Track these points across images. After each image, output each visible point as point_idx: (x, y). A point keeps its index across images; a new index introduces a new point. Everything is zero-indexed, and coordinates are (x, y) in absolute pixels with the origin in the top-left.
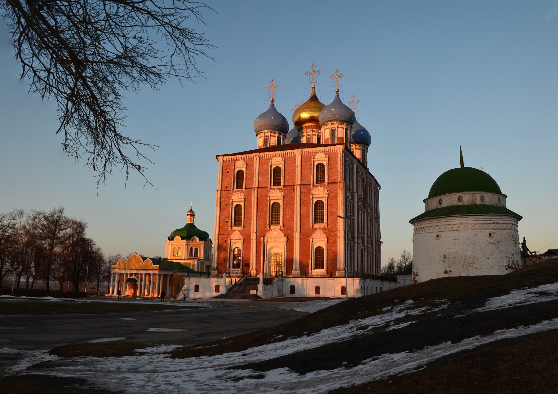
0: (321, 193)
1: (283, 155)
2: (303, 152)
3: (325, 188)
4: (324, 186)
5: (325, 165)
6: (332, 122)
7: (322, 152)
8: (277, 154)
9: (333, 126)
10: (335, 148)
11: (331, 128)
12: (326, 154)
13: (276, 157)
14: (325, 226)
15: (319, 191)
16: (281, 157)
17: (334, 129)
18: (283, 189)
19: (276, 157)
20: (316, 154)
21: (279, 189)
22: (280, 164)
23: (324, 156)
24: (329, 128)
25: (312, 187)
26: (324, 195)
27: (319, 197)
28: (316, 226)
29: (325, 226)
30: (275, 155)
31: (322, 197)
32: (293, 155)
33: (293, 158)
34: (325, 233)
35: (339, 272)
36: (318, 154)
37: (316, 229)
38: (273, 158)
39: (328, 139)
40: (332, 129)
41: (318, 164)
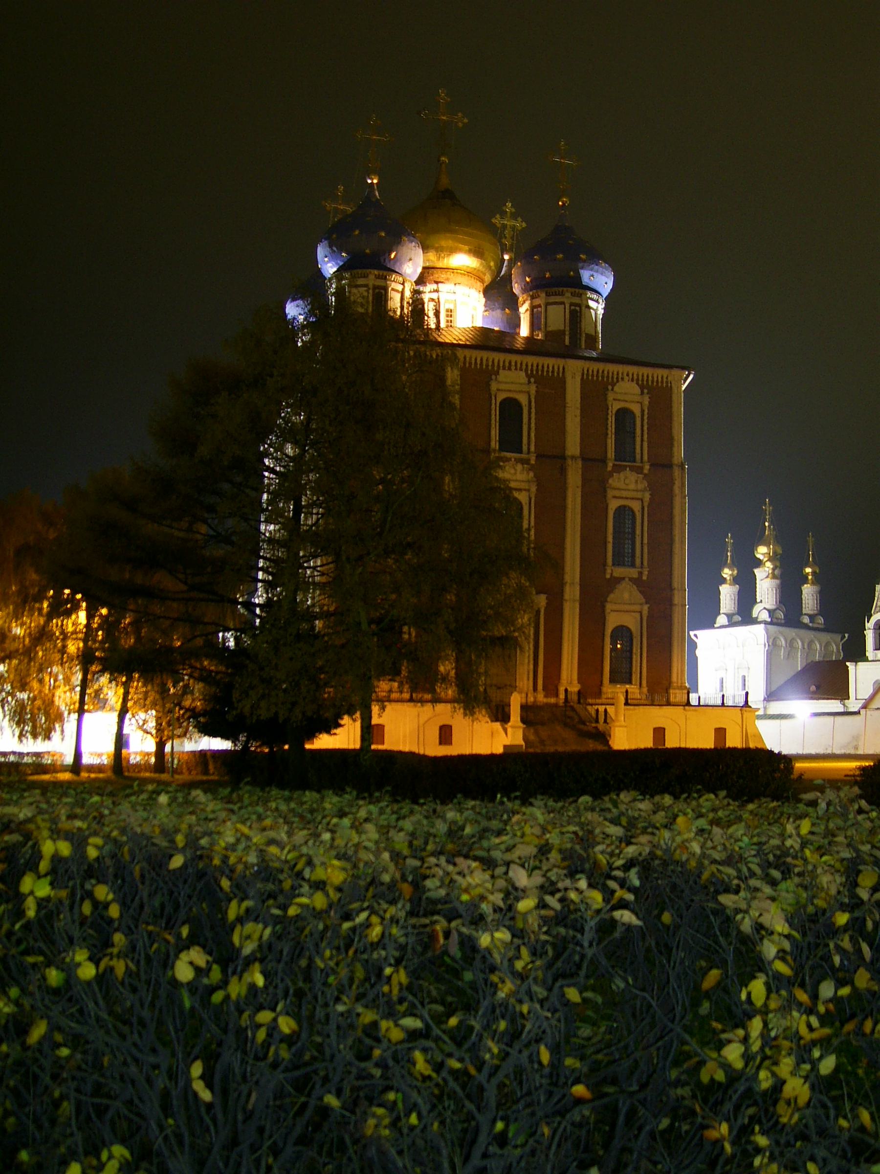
0: (632, 486)
1: (530, 367)
2: (586, 372)
3: (641, 476)
4: (639, 470)
5: (638, 413)
6: (577, 290)
7: (632, 380)
8: (513, 364)
9: (576, 300)
10: (665, 377)
11: (571, 304)
12: (642, 388)
13: (510, 369)
14: (641, 573)
15: (627, 481)
16: (524, 374)
17: (578, 308)
18: (533, 462)
19: (510, 369)
20: (618, 381)
21: (524, 462)
22: (521, 392)
23: (637, 390)
24: (563, 303)
25: (609, 469)
26: (639, 495)
27: (627, 498)
28: (619, 572)
29: (641, 573)
30: (507, 364)
31: (633, 499)
32: (558, 373)
33: (561, 383)
34: (640, 592)
35: (677, 691)
36: (621, 383)
37: (620, 580)
38: (501, 371)
39: (562, 333)
40: (573, 308)
41: (618, 411)
